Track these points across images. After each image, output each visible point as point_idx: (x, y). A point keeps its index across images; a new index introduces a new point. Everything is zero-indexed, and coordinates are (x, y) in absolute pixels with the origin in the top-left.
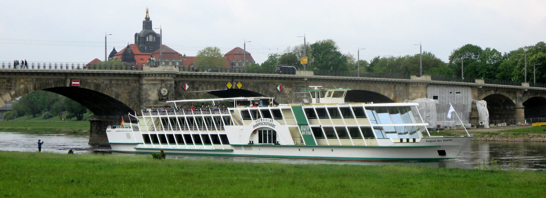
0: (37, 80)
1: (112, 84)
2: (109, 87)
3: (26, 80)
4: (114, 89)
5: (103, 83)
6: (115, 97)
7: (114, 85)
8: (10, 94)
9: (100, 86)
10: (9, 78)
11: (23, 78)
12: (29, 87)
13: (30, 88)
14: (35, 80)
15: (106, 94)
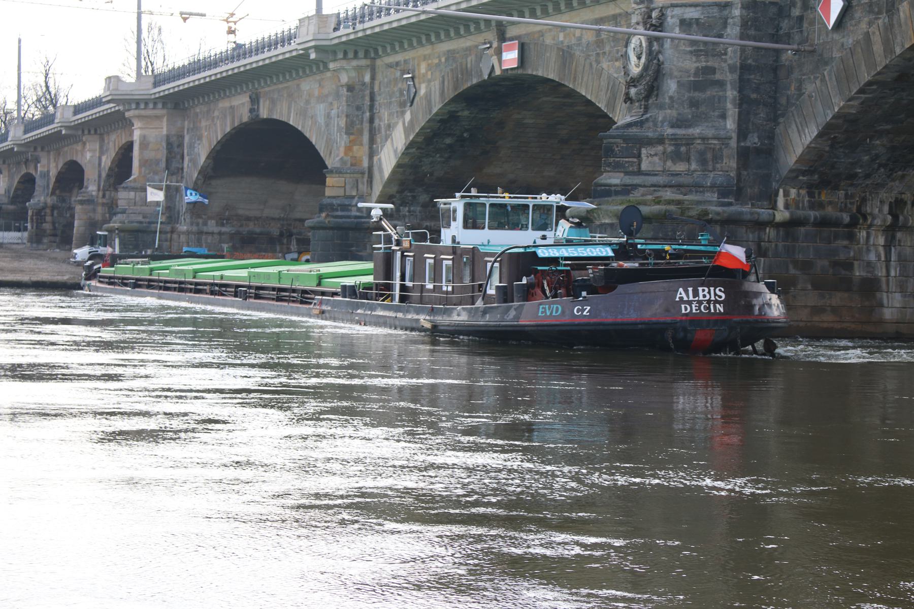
0: (450, 55)
1: (602, 40)
2: (593, 58)
3: (430, 61)
4: (605, 65)
5: (580, 39)
6: (607, 105)
7: (607, 49)
8: (404, 124)
9: (572, 56)
10: (405, 61)
11: (425, 58)
12: (433, 89)
13: (435, 92)
14: (443, 60)
15: (584, 94)
